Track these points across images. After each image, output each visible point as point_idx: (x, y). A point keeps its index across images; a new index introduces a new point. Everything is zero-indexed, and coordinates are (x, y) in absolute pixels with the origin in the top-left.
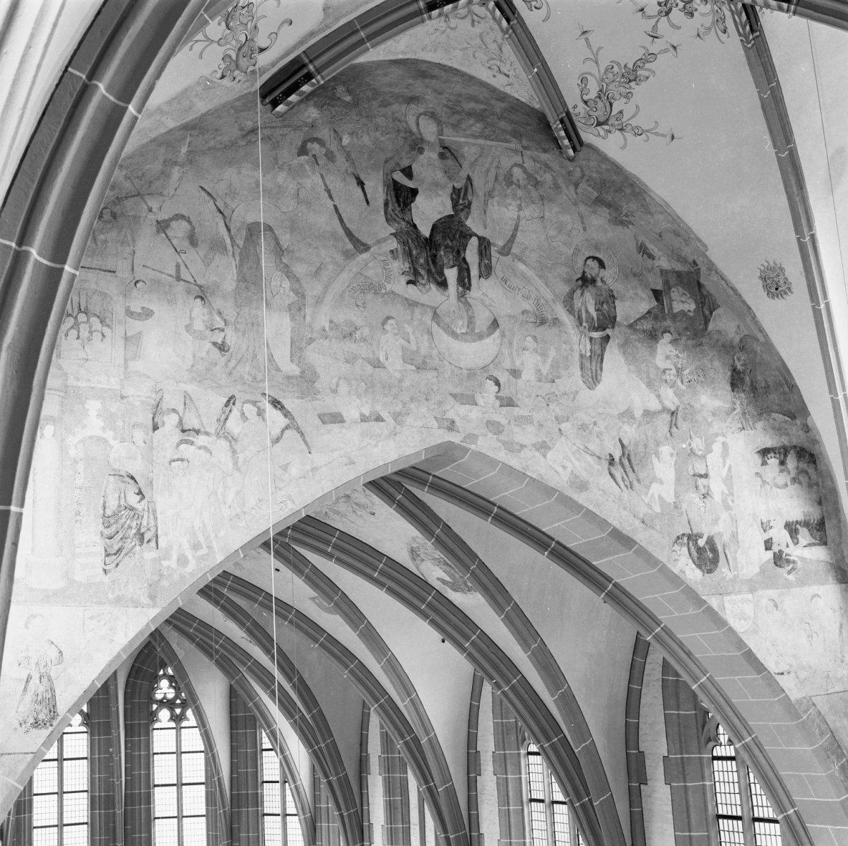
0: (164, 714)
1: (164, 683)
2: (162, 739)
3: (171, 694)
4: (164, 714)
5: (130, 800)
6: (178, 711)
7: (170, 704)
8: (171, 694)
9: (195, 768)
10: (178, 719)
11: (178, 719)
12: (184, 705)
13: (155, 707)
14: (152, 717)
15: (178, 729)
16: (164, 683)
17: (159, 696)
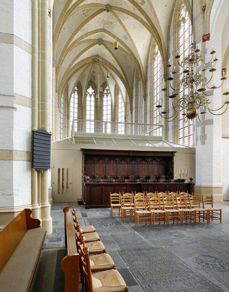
0: (105, 95)
1: (105, 91)
2: (105, 99)
3: (106, 92)
4: (105, 95)
5: (100, 107)
6: (107, 95)
7: (106, 94)
8: (106, 92)
9: (109, 103)
10: (107, 96)
11: (107, 96)
12: (108, 93)
13: (104, 94)
14: (103, 96)
15: (107, 97)
16: (105, 91)
17: (104, 93)
